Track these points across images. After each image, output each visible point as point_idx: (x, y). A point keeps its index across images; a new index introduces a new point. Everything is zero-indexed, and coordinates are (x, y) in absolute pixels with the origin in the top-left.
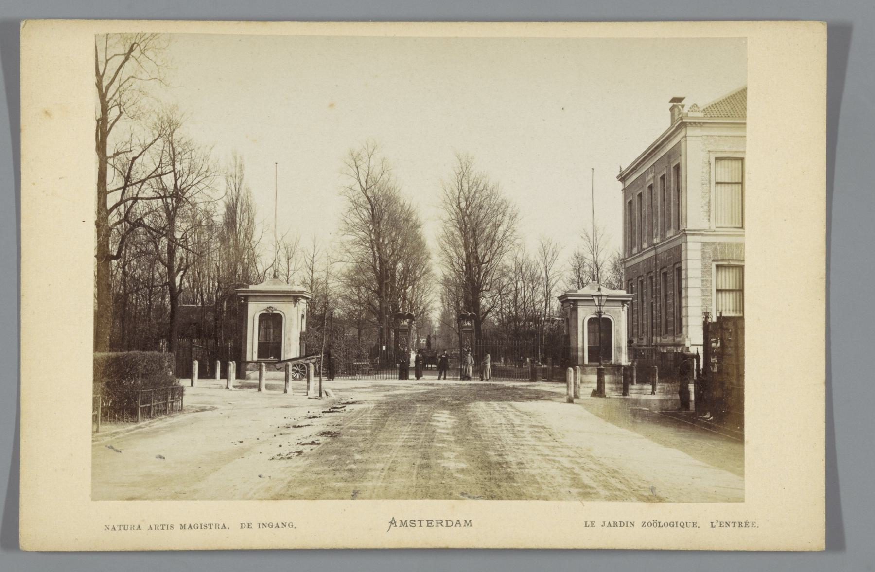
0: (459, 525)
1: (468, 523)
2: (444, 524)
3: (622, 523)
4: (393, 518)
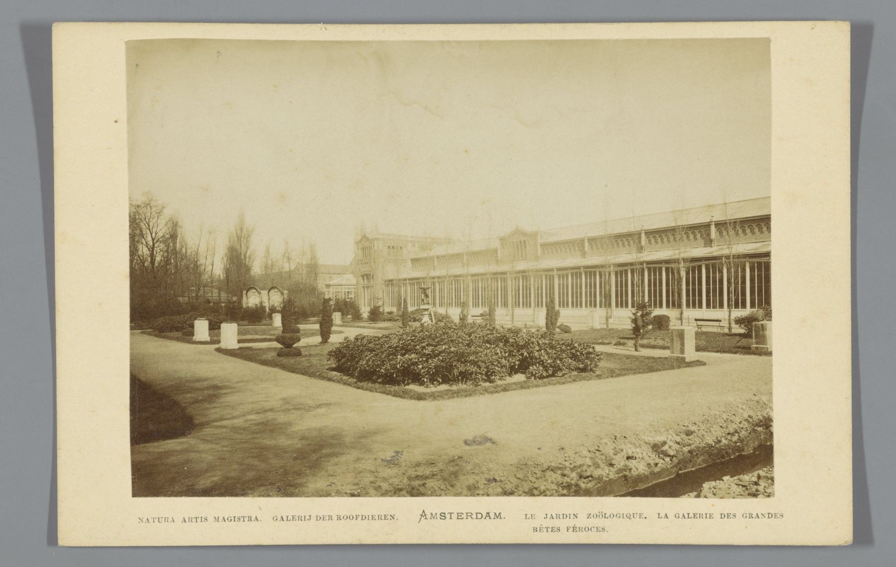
0: (489, 517)
1: (498, 516)
2: (474, 516)
3: (565, 516)
4: (424, 511)
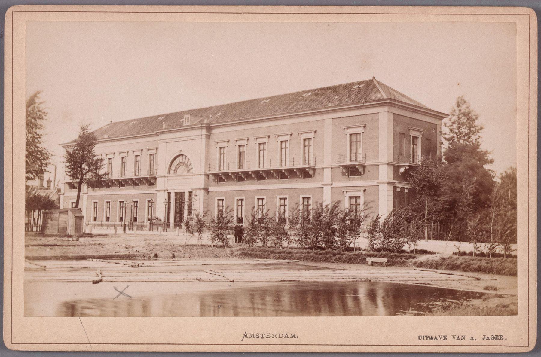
2: (278, 336)
4: (246, 332)
